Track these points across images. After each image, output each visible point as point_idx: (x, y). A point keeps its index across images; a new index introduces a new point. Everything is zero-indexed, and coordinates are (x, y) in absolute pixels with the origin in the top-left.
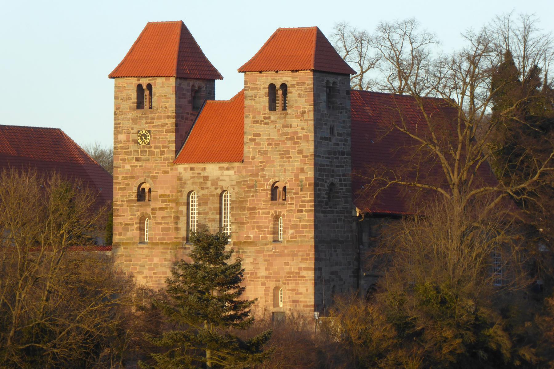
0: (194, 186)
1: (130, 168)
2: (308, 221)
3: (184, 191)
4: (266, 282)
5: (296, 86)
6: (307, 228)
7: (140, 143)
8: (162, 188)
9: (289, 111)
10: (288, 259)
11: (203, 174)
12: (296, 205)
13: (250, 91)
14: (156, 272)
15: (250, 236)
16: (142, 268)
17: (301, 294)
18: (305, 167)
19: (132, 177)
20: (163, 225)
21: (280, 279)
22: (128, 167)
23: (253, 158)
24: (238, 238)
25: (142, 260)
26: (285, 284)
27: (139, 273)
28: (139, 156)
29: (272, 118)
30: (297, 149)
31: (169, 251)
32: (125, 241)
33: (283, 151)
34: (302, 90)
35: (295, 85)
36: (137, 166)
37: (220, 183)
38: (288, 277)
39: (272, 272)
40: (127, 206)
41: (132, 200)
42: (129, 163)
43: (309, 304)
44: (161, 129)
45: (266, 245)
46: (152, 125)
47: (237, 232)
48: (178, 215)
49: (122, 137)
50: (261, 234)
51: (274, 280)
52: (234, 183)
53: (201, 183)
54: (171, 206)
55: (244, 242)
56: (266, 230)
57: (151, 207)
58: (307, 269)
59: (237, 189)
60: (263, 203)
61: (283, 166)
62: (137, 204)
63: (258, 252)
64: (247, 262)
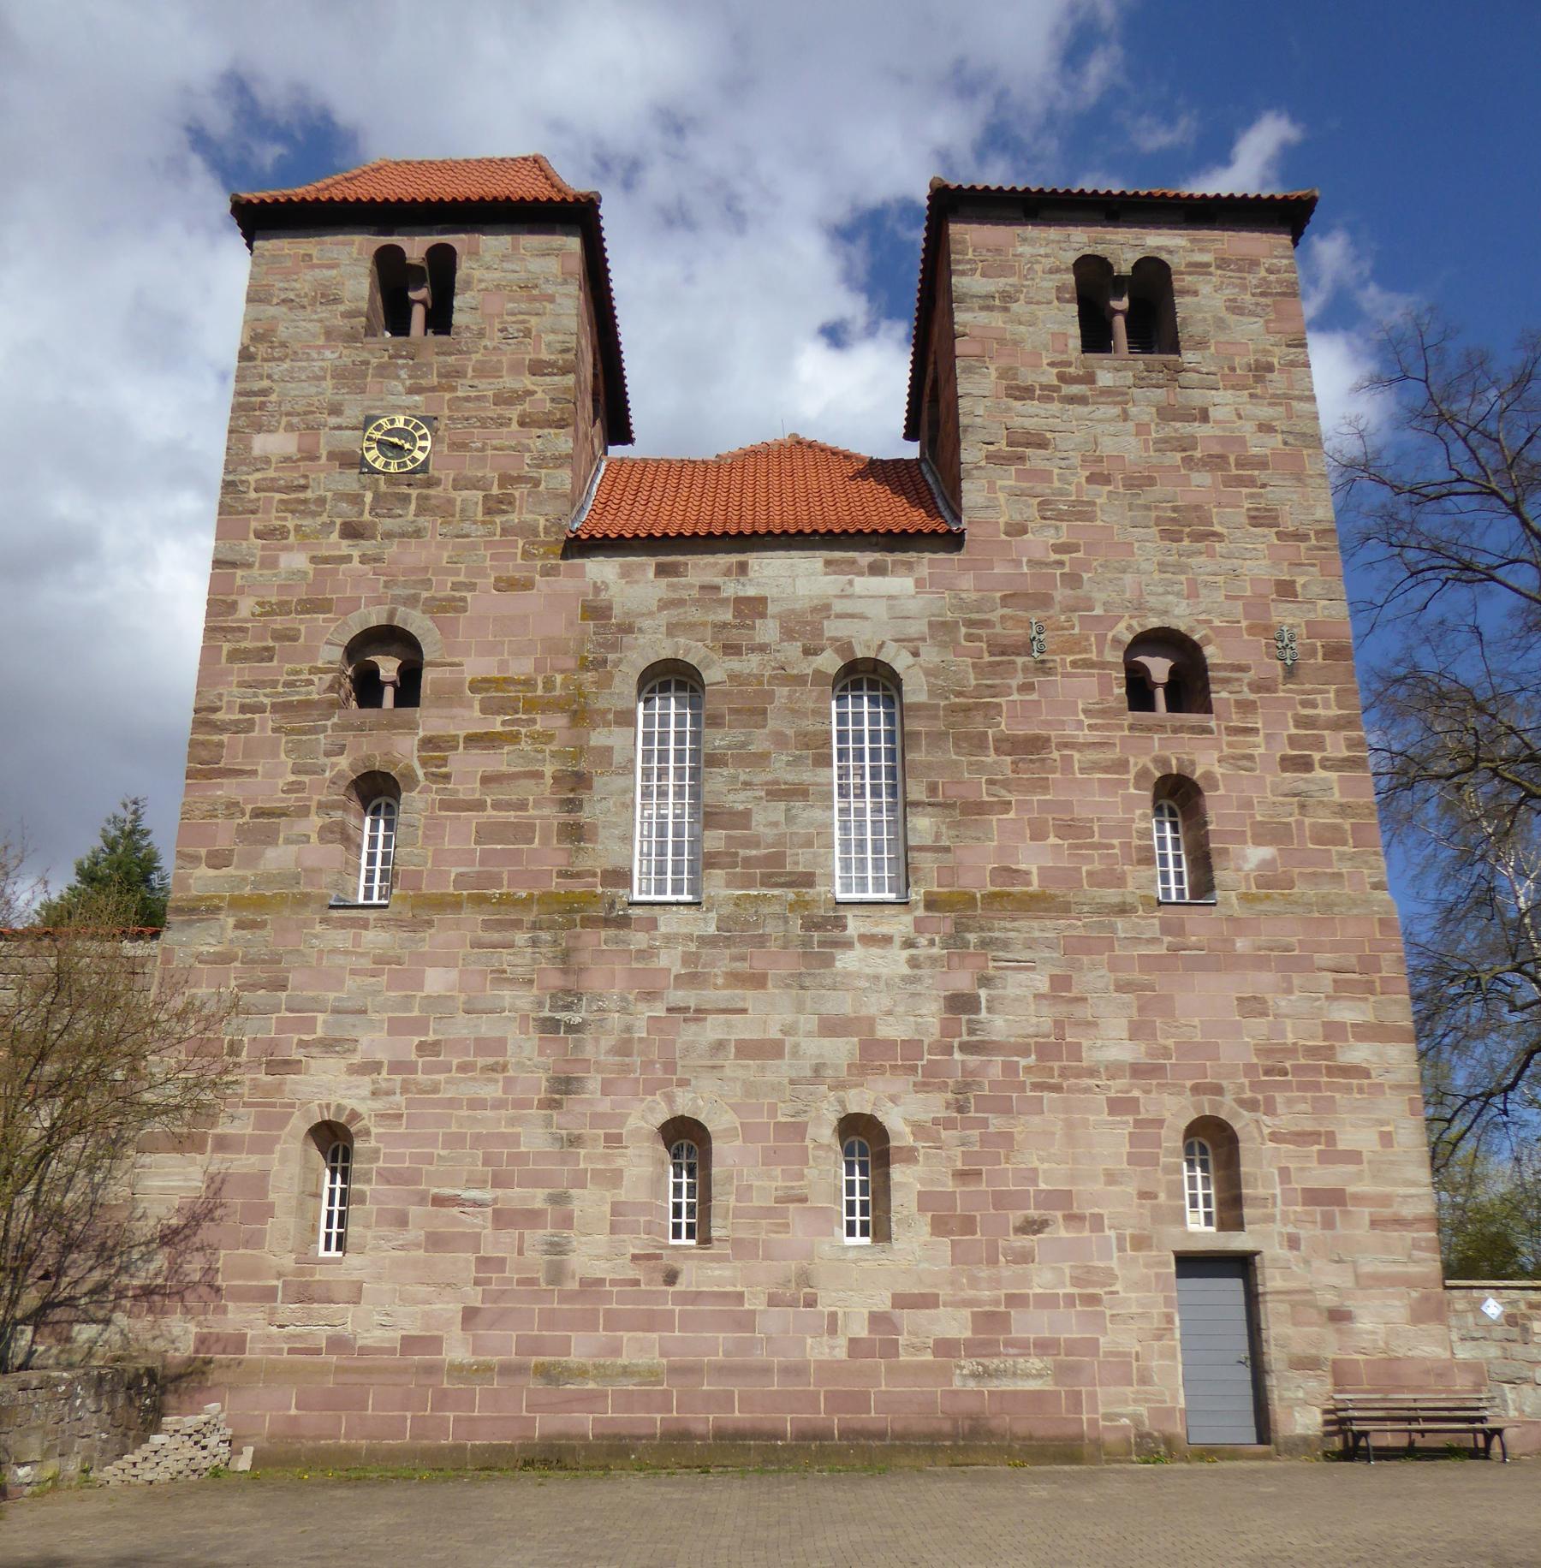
0: (682, 640)
1: (310, 568)
2: (1343, 810)
3: (620, 661)
4: (1136, 1093)
5: (1212, 269)
6: (1345, 843)
7: (378, 465)
8: (491, 649)
9: (1188, 357)
10: (1263, 981)
11: (731, 589)
12: (1268, 736)
13: (977, 275)
14: (436, 1043)
15: (1023, 867)
16: (350, 1019)
17: (1354, 1157)
18: (1300, 580)
19: (314, 606)
20: (490, 812)
21: (1225, 1083)
22: (296, 560)
23: (1018, 530)
24: (949, 873)
25: (350, 983)
26: (1252, 1105)
27: (329, 1045)
28: (367, 517)
29: (1105, 379)
30: (1247, 505)
31: (521, 937)
32: (247, 891)
33: (1175, 509)
34: (1244, 288)
35: (1208, 265)
36: (348, 559)
37: (832, 628)
38: (1267, 1072)
39: (1170, 1042)
40: (274, 730)
41: (307, 704)
42: (302, 547)
43: (1408, 1211)
44: (493, 411)
45: (1123, 910)
46: (448, 396)
47: (947, 850)
48: (583, 766)
49: (274, 444)
50: (1089, 859)
51: (1189, 1083)
52: (918, 628)
53: (725, 625)
54: (538, 727)
55: (991, 898)
56: (1116, 842)
57: (421, 734)
58: (1365, 1033)
59: (931, 655)
60: (1087, 722)
61: (1181, 569)
62: (335, 719)
63: (1076, 947)
64: (1011, 991)
